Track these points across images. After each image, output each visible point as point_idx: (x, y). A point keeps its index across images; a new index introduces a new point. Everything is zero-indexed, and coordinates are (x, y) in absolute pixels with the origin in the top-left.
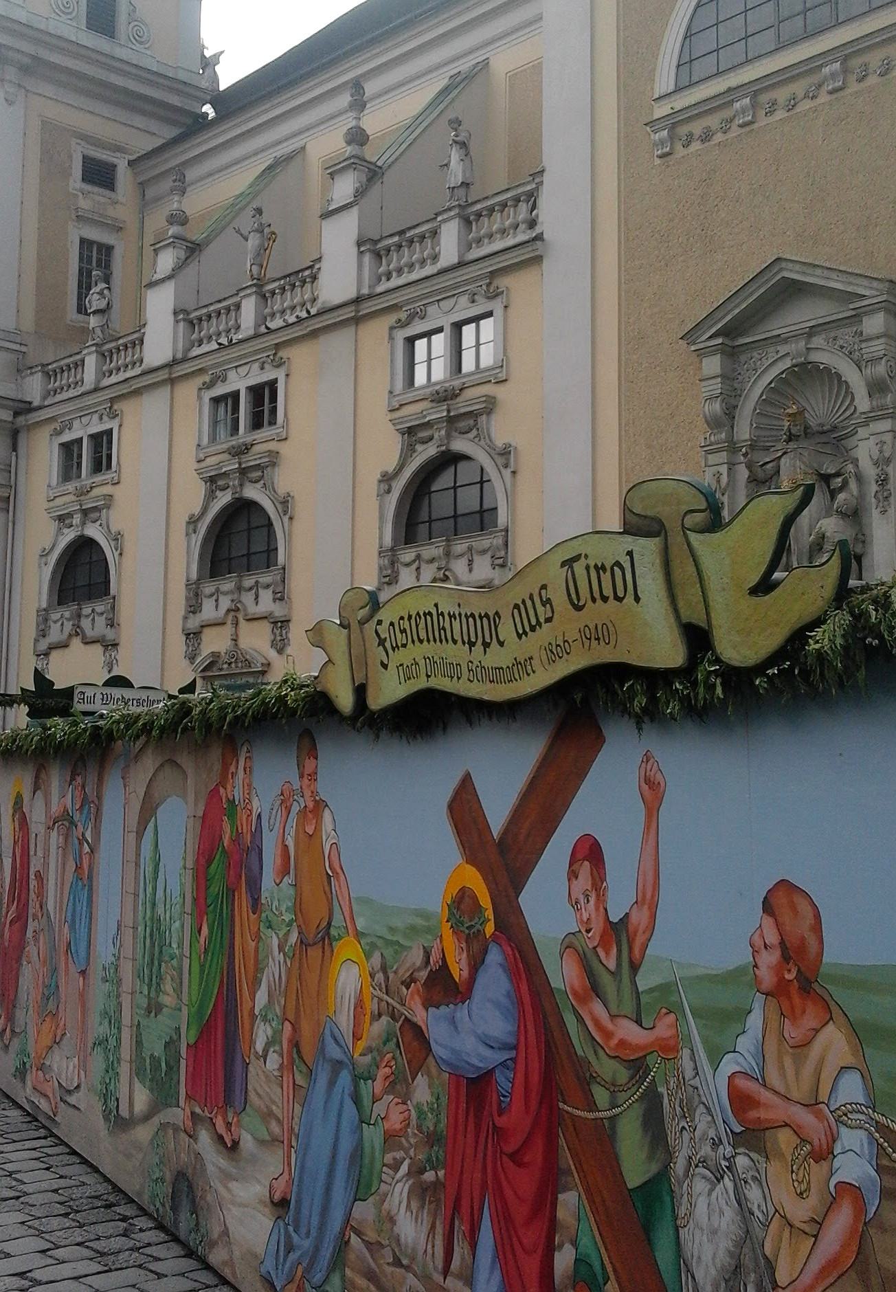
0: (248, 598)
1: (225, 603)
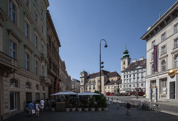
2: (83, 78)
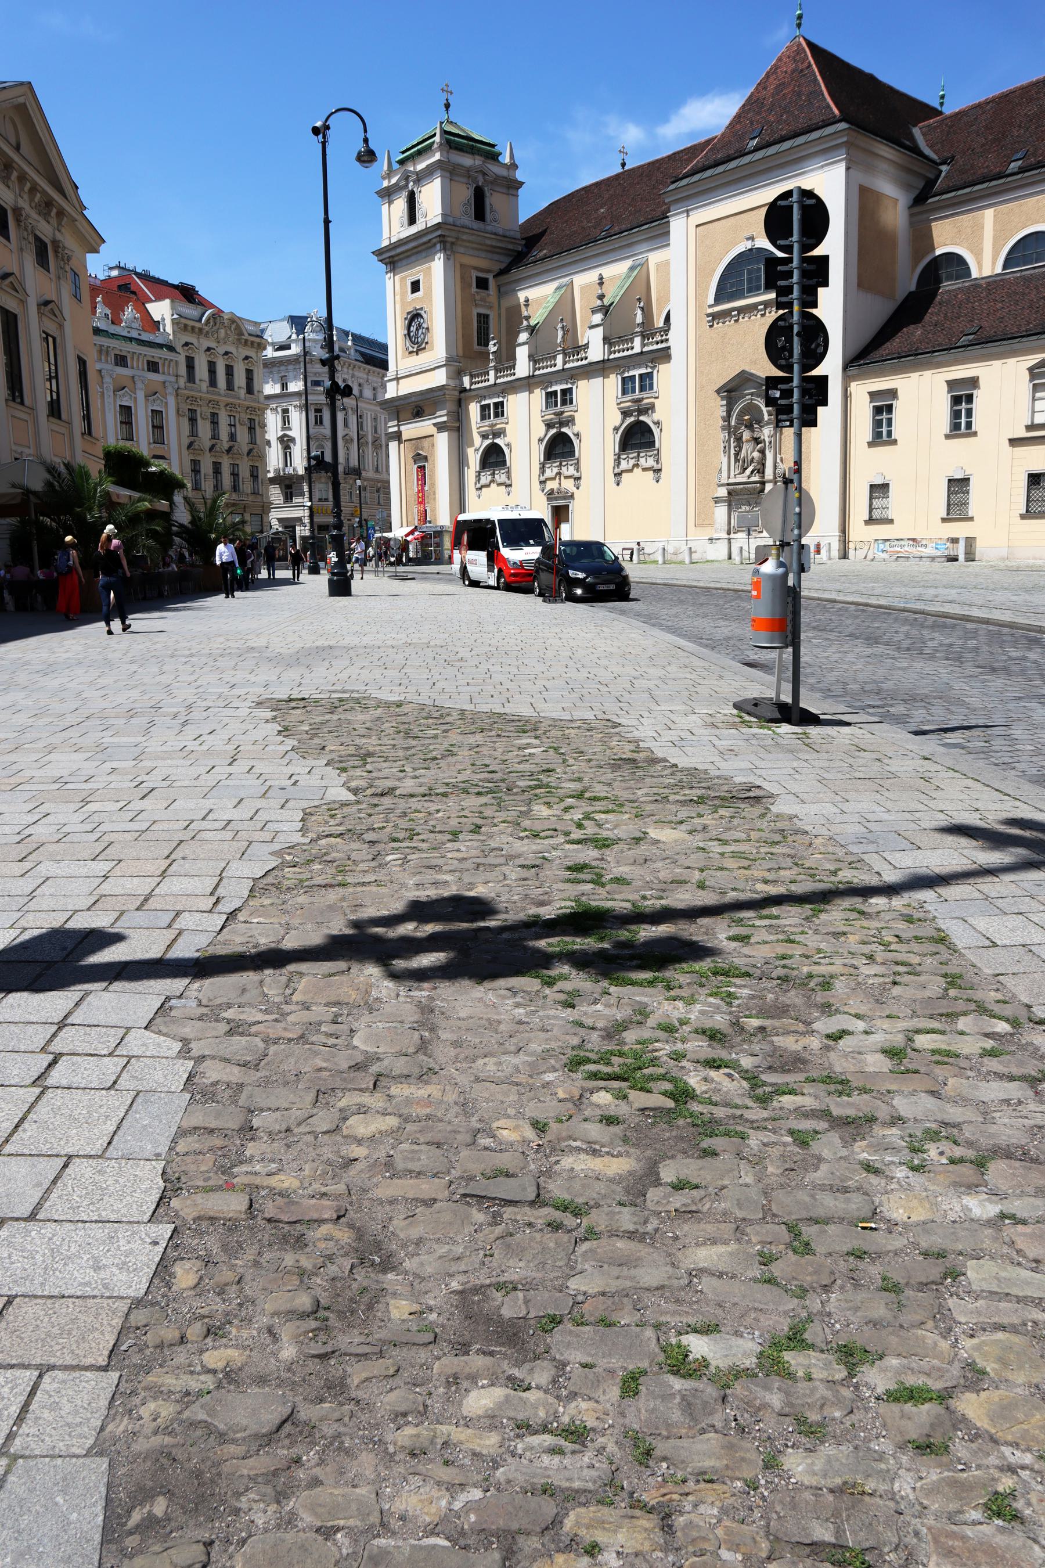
1: (555, 470)
2: (435, 271)
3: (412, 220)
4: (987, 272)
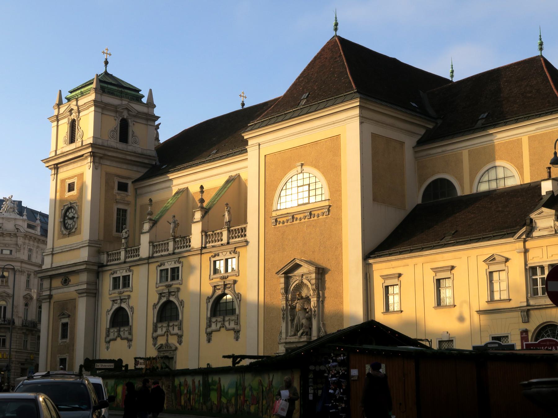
0: (171, 329)
1: (164, 330)
3: (72, 140)
4: (467, 192)
